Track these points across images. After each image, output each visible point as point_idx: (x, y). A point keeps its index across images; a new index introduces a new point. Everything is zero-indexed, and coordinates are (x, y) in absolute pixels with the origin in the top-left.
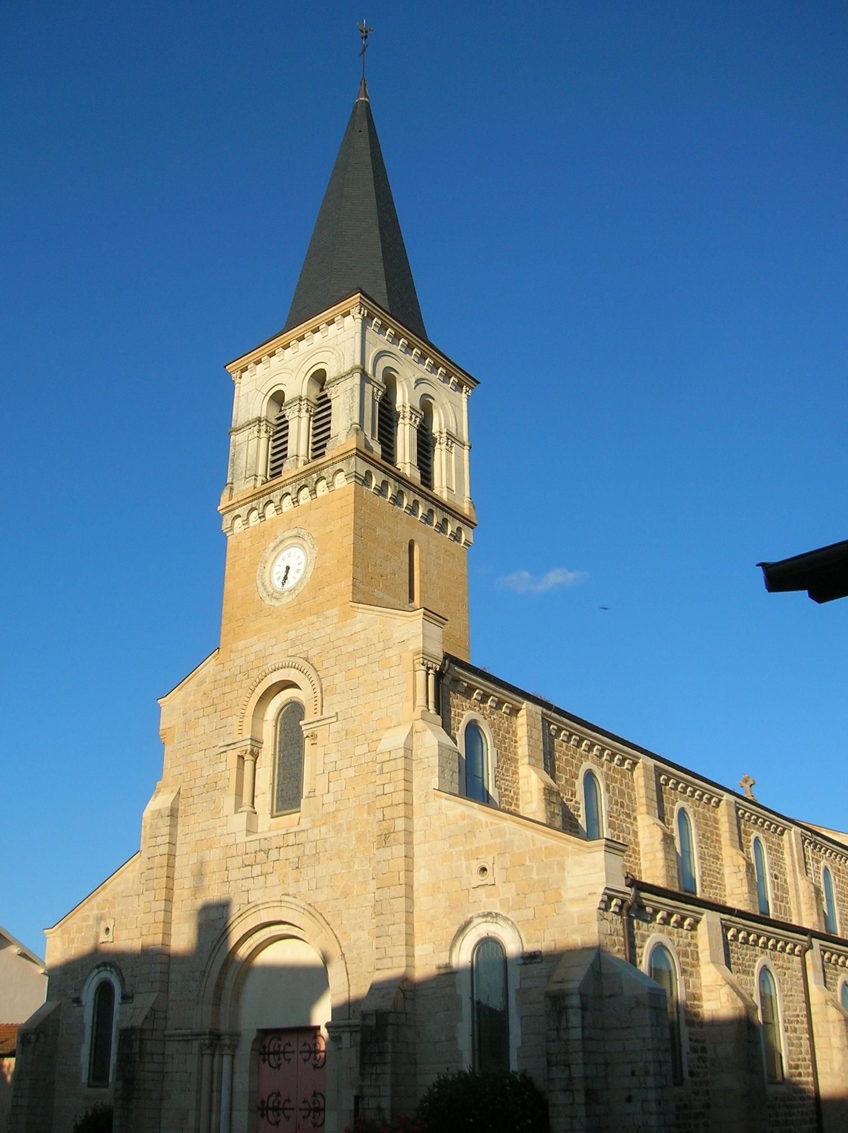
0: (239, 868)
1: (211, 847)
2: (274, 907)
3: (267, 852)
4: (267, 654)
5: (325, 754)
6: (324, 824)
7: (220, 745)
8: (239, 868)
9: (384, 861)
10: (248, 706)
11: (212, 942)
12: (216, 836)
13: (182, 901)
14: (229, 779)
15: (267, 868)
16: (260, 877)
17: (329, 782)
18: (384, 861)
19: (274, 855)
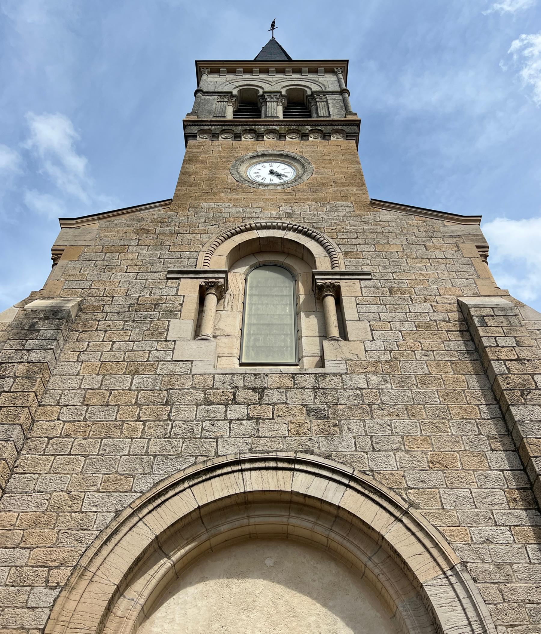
0: (197, 405)
1: (137, 373)
2: (276, 469)
3: (261, 391)
4: (247, 215)
5: (357, 304)
6: (375, 373)
7: (171, 269)
8: (197, 405)
9: (531, 421)
10: (221, 245)
11: (118, 513)
12: (148, 361)
13: (50, 438)
14: (181, 305)
15: (256, 411)
16: (244, 422)
17: (372, 330)
18: (531, 421)
19: (273, 396)
